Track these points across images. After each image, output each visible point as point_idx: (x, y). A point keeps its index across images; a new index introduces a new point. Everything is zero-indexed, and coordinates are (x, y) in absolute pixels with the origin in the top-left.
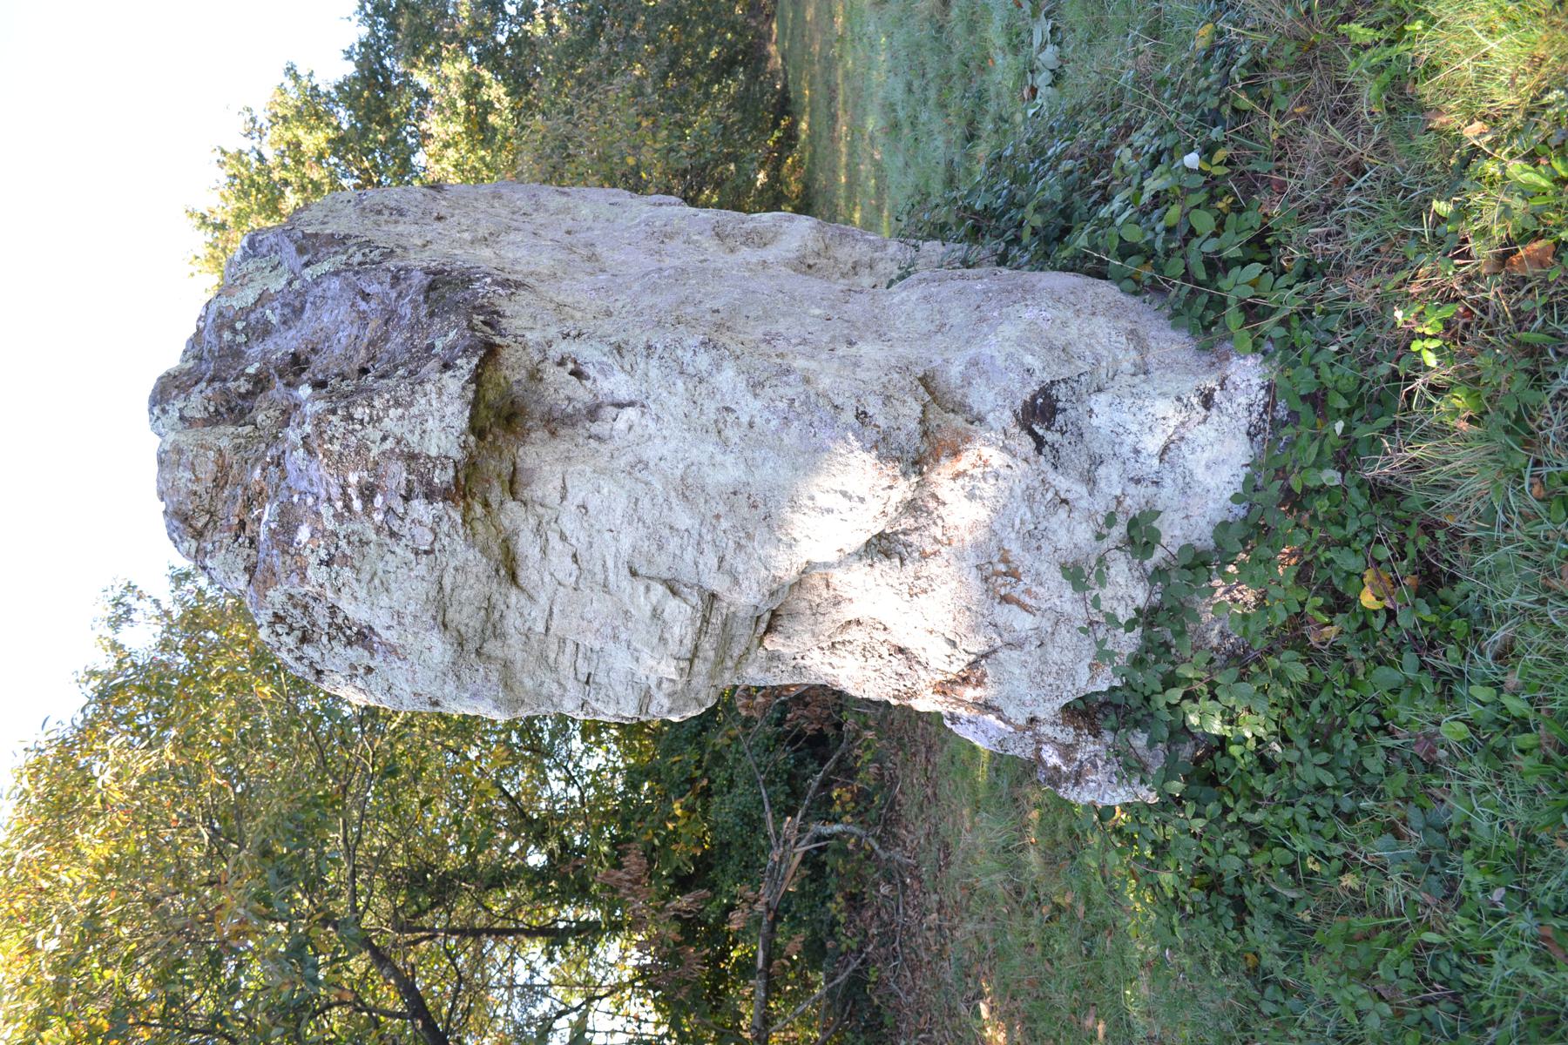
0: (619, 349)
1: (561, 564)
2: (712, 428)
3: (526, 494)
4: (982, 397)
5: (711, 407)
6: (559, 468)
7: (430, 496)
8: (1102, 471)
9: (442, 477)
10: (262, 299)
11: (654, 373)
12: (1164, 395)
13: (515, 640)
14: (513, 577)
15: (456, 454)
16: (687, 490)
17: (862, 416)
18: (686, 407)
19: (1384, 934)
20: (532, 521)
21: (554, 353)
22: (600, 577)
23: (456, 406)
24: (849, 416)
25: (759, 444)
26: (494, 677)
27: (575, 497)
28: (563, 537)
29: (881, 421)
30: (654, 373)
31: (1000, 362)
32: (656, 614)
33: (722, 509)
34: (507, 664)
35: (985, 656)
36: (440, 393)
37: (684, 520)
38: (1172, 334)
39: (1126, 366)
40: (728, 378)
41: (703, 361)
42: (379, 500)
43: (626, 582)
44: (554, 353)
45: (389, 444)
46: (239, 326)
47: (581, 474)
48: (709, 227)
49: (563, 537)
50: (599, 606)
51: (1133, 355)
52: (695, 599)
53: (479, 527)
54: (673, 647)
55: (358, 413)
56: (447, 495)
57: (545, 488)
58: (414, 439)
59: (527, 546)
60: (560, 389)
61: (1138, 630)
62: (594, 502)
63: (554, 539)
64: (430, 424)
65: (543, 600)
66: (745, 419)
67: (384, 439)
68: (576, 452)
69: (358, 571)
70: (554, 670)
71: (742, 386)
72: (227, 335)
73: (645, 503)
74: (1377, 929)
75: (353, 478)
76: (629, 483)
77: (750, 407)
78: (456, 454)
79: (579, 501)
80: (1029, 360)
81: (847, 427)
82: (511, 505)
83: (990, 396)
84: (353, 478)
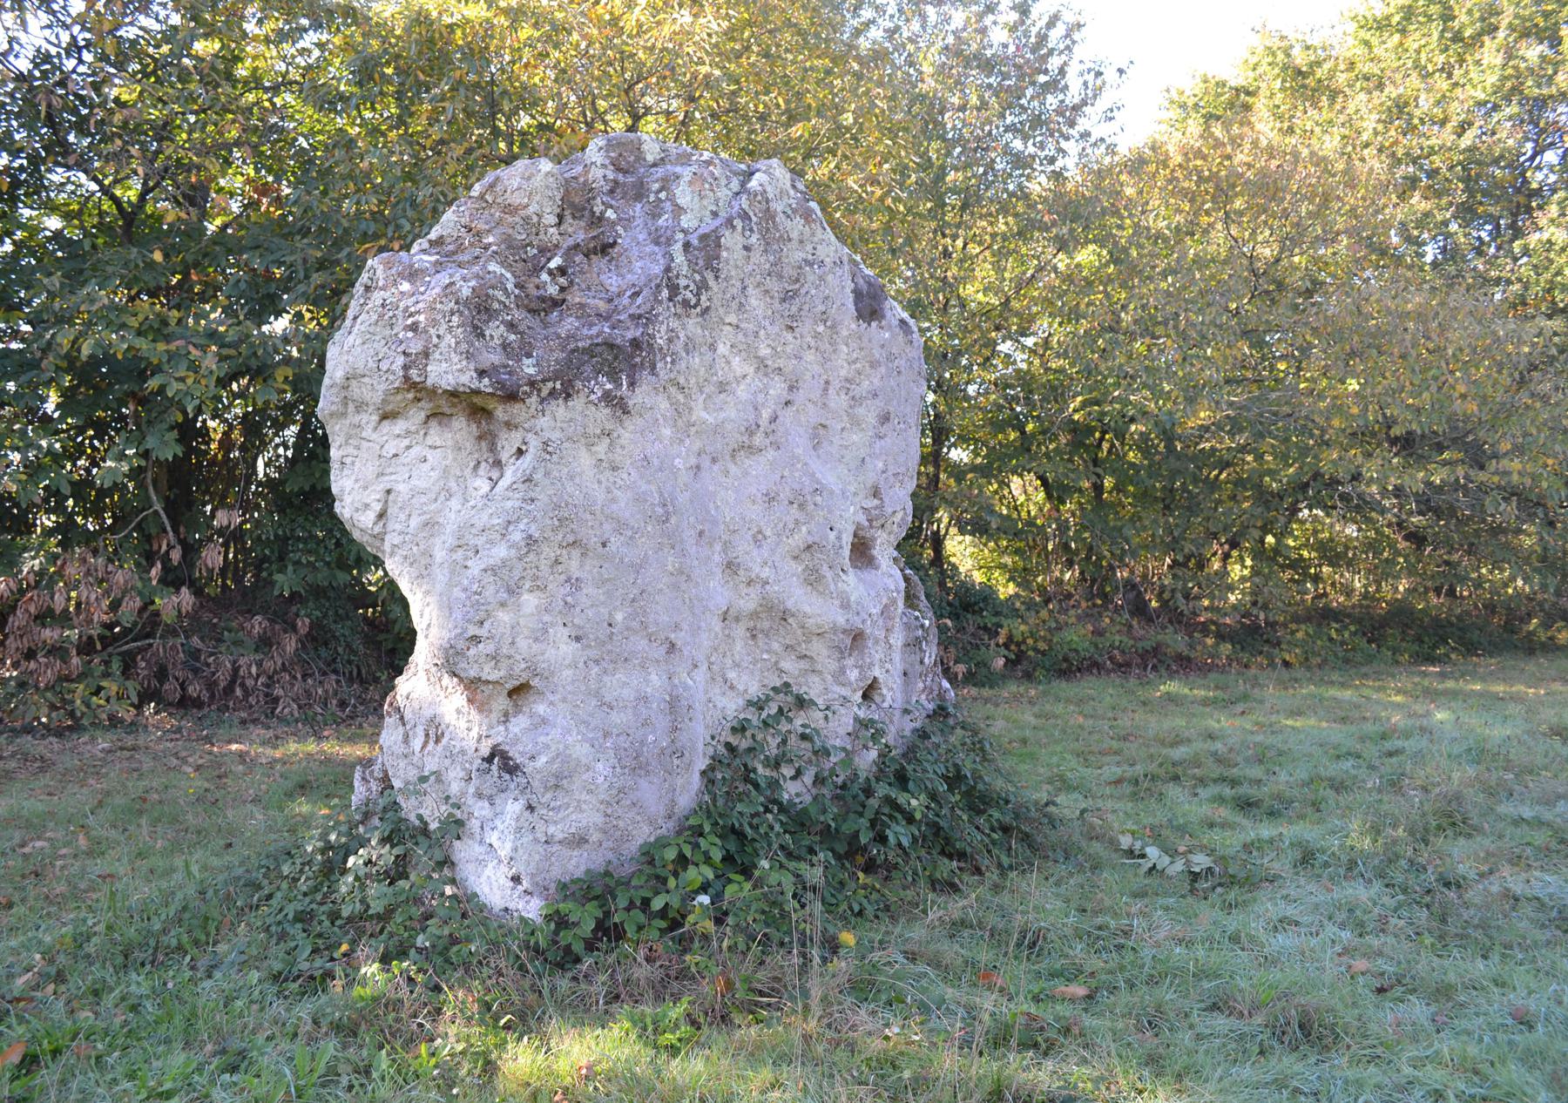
0: (528, 480)
1: (390, 449)
2: (461, 542)
3: (433, 423)
4: (519, 724)
5: (480, 541)
6: (450, 443)
7: (406, 367)
8: (486, 804)
9: (413, 373)
10: (679, 210)
11: (509, 504)
12: (515, 849)
13: (356, 419)
14: (385, 417)
15: (429, 382)
16: (430, 525)
17: (475, 639)
18: (479, 525)
19: (203, 938)
20: (413, 428)
21: (530, 437)
22: (388, 471)
23: (452, 382)
24: (473, 630)
25: (452, 572)
26: (334, 408)
27: (430, 454)
28: (408, 447)
29: (472, 652)
30: (509, 504)
31: (542, 739)
32: (367, 506)
33: (422, 547)
34: (344, 415)
35: (402, 718)
36: (460, 370)
37: (415, 522)
38: (583, 868)
39: (551, 830)
40: (501, 552)
41: (517, 536)
42: (410, 334)
43: (382, 487)
44: (530, 437)
45: (435, 340)
46: (663, 195)
47: (445, 458)
48: (817, 539)
49: (408, 447)
50: (370, 470)
51: (560, 836)
52: (377, 529)
53: (399, 397)
54: (356, 516)
55: (455, 319)
56: (406, 378)
57: (436, 435)
58: (437, 356)
59: (400, 426)
60: (508, 443)
61: (417, 823)
62: (426, 467)
63: (406, 442)
64: (444, 365)
65: (374, 436)
66: (469, 563)
67: (439, 337)
68: (464, 454)
69: (376, 323)
70: (347, 443)
71: (492, 562)
72: (656, 186)
73: (424, 499)
74: (208, 935)
75: (422, 318)
76: (436, 489)
77: (476, 566)
78: (429, 382)
79: (429, 457)
80: (543, 759)
81: (465, 630)
82: (423, 415)
83: (516, 730)
84: (422, 318)
